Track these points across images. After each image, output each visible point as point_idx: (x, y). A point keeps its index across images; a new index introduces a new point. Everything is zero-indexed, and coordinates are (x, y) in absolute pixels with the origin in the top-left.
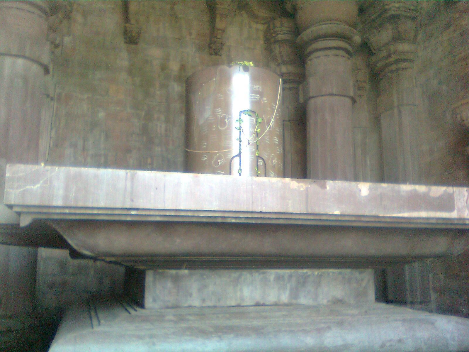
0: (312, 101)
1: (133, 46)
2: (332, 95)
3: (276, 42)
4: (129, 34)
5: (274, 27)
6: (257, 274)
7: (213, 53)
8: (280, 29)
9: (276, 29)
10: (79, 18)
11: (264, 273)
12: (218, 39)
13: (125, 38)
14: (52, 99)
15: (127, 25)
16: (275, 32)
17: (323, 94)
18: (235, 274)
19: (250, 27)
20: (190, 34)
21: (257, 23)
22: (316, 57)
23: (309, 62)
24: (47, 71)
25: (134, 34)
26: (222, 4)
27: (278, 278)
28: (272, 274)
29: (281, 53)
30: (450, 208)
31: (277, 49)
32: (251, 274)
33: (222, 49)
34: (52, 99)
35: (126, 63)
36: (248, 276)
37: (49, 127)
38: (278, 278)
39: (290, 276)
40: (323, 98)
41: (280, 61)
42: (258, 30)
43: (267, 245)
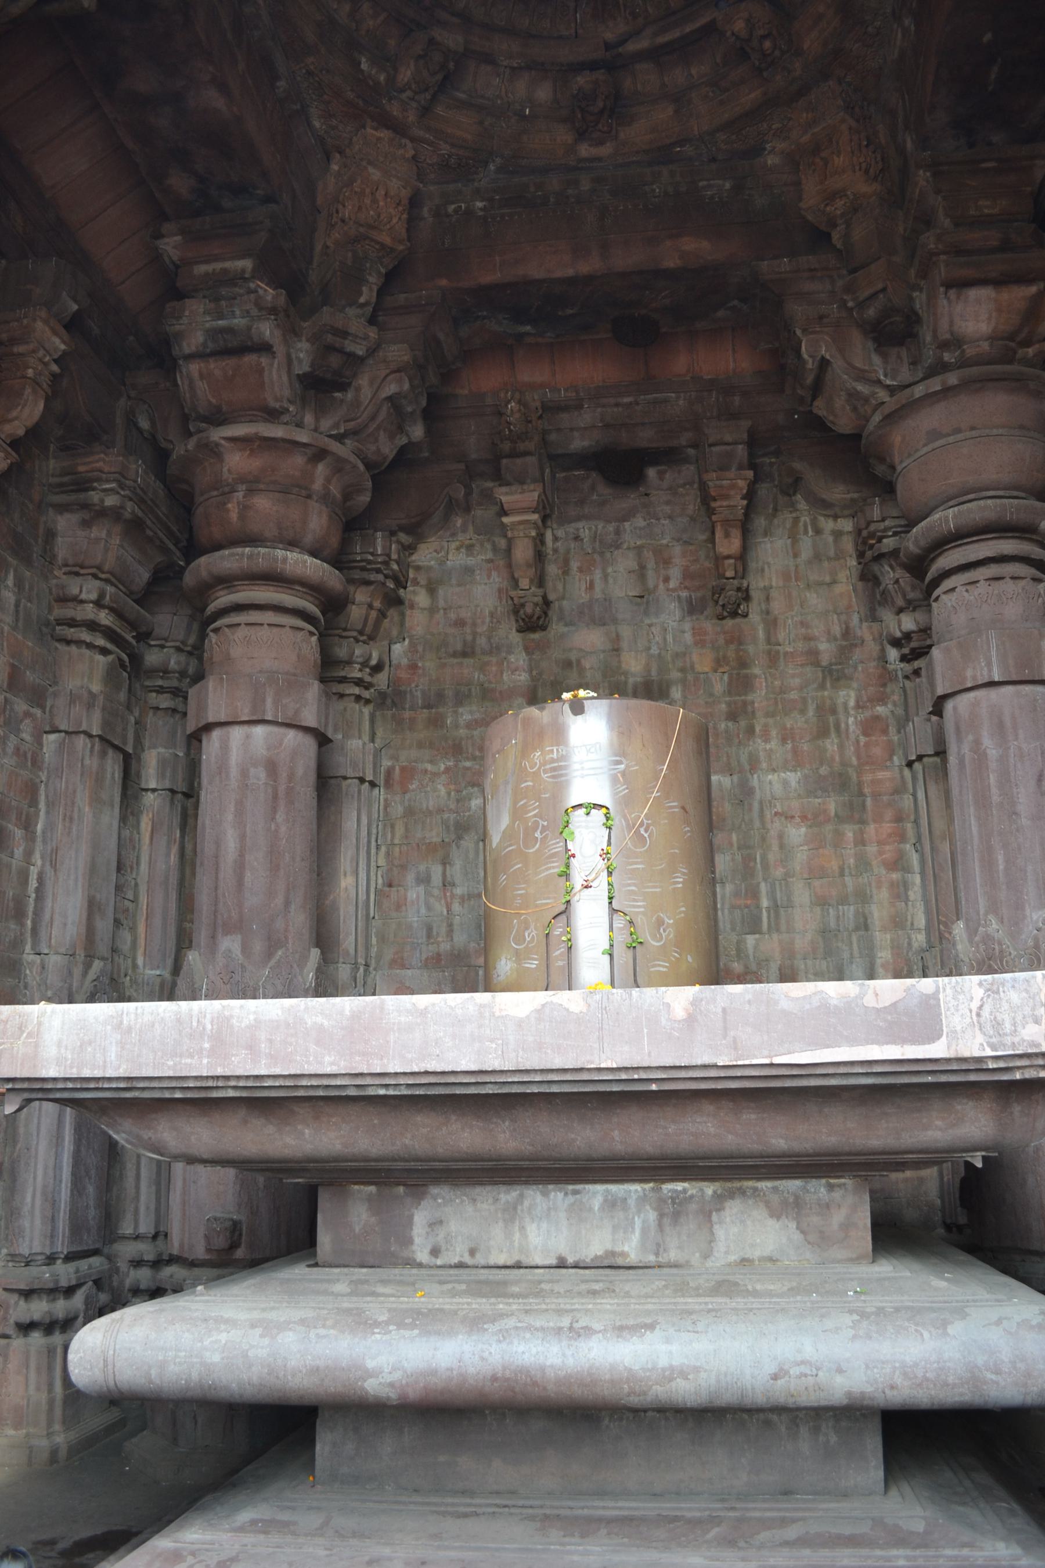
0: (949, 706)
1: (536, 636)
2: (991, 684)
3: (879, 557)
4: (522, 612)
5: (868, 524)
6: (560, 1195)
7: (725, 614)
8: (882, 526)
9: (873, 527)
10: (422, 599)
11: (576, 1192)
12: (728, 579)
13: (517, 621)
14: (373, 784)
15: (513, 593)
16: (872, 535)
17: (969, 685)
18: (507, 1195)
19: (818, 531)
20: (667, 580)
21: (836, 517)
22: (945, 593)
23: (934, 604)
24: (323, 740)
25: (529, 609)
26: (726, 497)
27: (612, 1204)
28: (597, 1193)
29: (897, 582)
30: (933, 1036)
31: (890, 575)
32: (546, 1194)
33: (747, 598)
34: (373, 784)
35: (523, 677)
36: (539, 1198)
37: (373, 844)
38: (612, 1204)
39: (643, 1199)
40: (972, 695)
41: (900, 602)
42: (838, 534)
43: (505, 1137)
